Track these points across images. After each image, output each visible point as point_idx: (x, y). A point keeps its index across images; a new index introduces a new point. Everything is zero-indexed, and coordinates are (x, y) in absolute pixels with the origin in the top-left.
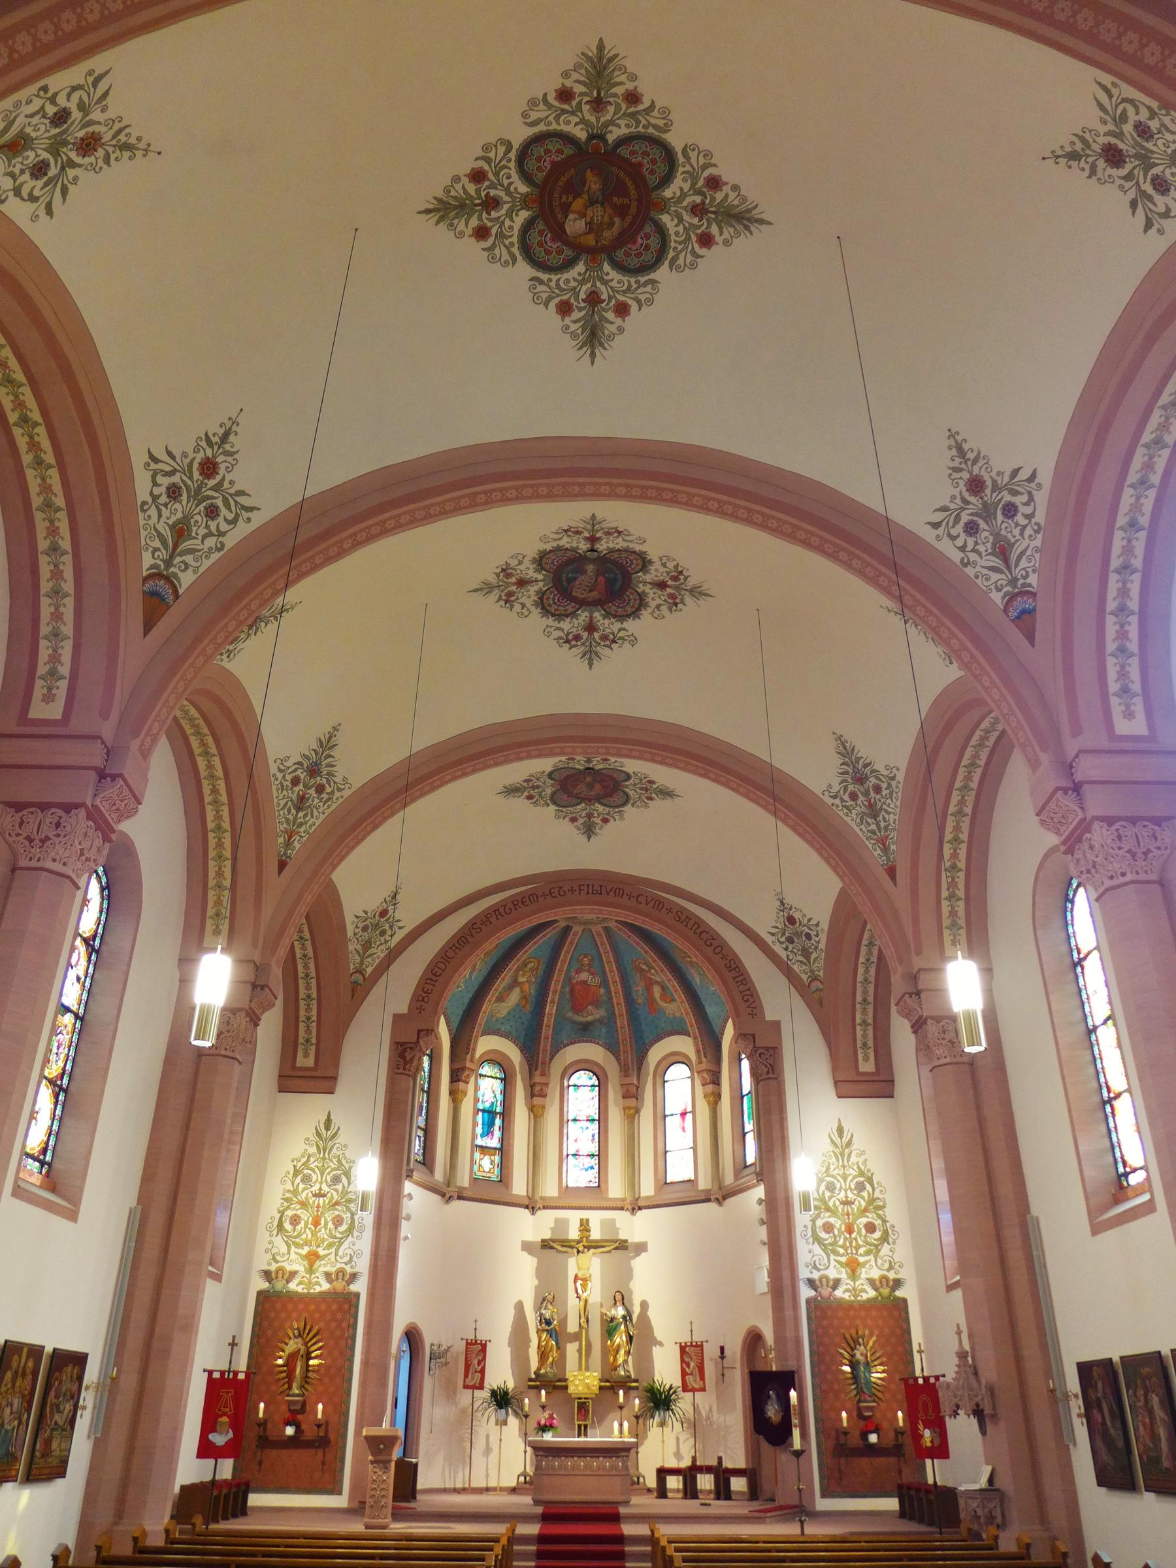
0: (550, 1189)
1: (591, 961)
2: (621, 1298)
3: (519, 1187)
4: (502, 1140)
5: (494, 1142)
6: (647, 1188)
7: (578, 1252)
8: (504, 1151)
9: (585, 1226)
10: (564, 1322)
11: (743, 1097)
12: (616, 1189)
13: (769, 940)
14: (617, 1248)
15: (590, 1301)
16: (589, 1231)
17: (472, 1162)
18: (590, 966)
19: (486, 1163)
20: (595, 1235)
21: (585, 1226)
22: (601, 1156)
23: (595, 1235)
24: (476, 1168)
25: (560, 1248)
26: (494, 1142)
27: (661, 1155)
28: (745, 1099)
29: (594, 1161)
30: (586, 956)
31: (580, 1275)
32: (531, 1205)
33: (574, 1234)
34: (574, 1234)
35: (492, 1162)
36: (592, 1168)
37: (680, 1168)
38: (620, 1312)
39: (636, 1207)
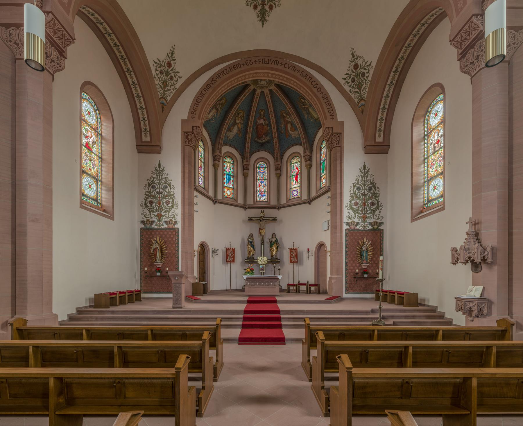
1: (264, 113)
13: (342, 82)
18: (264, 116)
30: (262, 110)
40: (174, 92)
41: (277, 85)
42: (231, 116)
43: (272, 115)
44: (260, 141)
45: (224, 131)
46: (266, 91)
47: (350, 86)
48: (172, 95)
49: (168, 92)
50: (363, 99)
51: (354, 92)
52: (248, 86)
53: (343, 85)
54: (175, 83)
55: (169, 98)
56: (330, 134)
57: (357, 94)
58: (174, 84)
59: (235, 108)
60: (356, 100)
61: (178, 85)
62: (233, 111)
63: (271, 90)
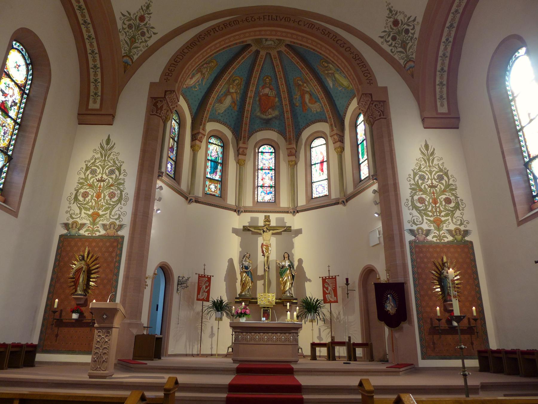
0: (248, 203)
2: (288, 256)
3: (231, 200)
4: (221, 177)
5: (217, 177)
6: (302, 201)
7: (264, 231)
8: (222, 182)
9: (267, 219)
10: (256, 269)
11: (358, 145)
12: (284, 203)
13: (379, 41)
14: (285, 231)
15: (270, 259)
16: (270, 222)
17: (205, 186)
19: (212, 187)
20: (273, 223)
21: (267, 219)
22: (276, 187)
23: (273, 223)
24: (206, 189)
25: (253, 230)
26: (217, 177)
27: (310, 184)
28: (360, 146)
29: (272, 190)
31: (264, 244)
32: (238, 210)
33: (261, 223)
34: (261, 223)
35: (216, 187)
36: (271, 193)
37: (320, 189)
38: (287, 263)
39: (295, 211)
40: (144, 50)
41: (288, 46)
42: (223, 82)
43: (282, 82)
44: (264, 117)
45: (212, 100)
46: (274, 53)
47: (390, 45)
48: (141, 53)
49: (135, 50)
50: (410, 60)
51: (398, 52)
52: (249, 46)
53: (380, 44)
54: (147, 39)
55: (135, 57)
56: (368, 103)
57: (402, 55)
58: (146, 41)
59: (229, 73)
60: (402, 62)
61: (150, 43)
62: (226, 76)
63: (279, 52)
